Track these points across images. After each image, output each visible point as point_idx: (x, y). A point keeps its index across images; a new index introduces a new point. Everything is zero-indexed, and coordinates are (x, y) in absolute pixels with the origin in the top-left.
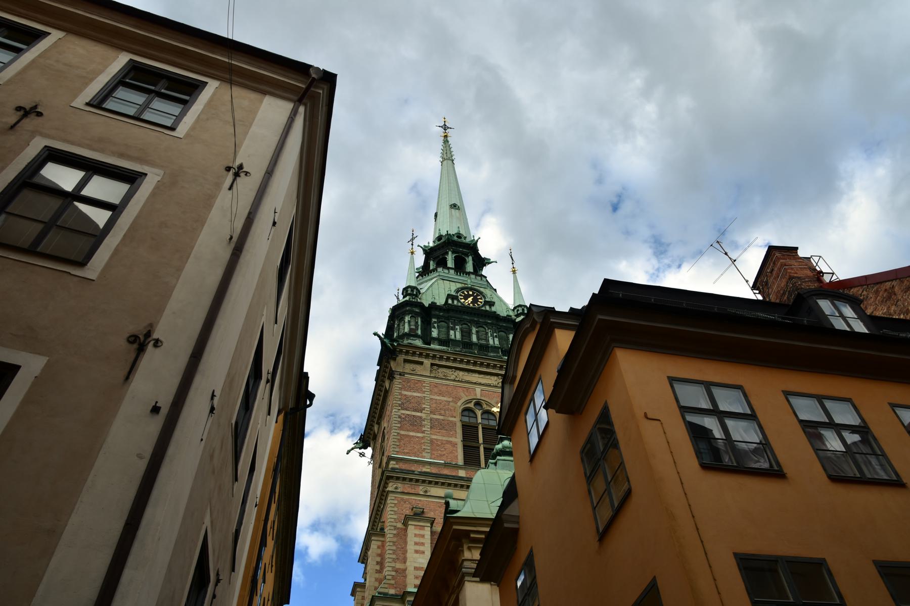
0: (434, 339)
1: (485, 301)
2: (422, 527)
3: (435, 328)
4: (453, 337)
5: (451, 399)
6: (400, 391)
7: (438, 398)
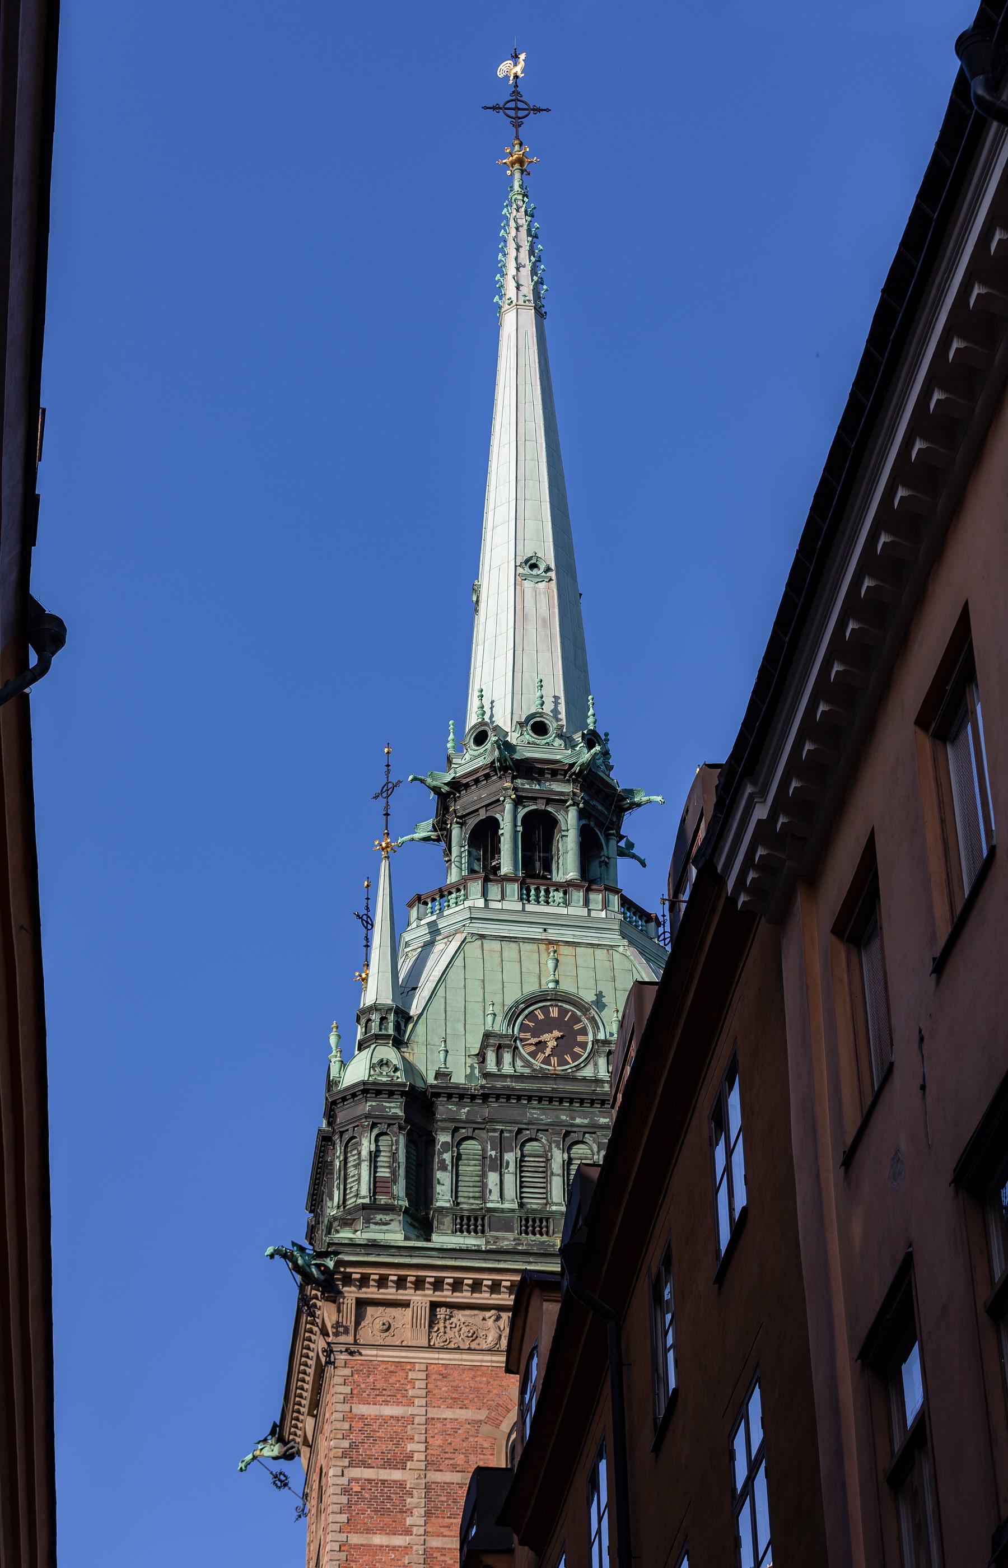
0: (442, 1209)
1: (596, 1041)
3: (443, 1168)
5: (482, 1415)
6: (346, 1407)
7: (448, 1414)
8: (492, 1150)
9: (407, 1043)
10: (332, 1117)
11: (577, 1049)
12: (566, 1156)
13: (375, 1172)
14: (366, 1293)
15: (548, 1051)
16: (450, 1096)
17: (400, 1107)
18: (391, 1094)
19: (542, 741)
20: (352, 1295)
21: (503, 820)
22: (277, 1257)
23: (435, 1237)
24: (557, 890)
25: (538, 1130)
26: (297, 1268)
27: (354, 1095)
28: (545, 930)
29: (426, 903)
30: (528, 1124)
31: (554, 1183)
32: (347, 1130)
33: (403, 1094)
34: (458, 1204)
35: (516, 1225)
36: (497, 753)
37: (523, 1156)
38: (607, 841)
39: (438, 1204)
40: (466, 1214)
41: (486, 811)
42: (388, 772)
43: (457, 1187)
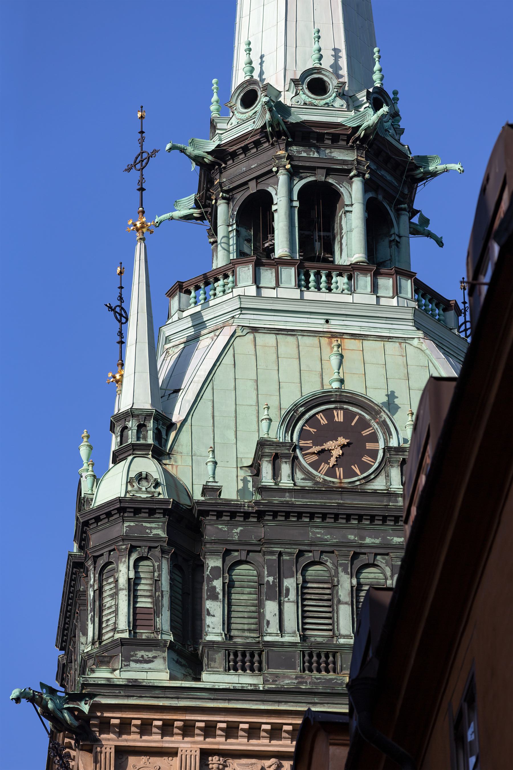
1: (387, 449)
3: (214, 597)
8: (269, 575)
9: (169, 454)
10: (84, 540)
11: (366, 459)
12: (354, 581)
13: (135, 602)
14: (127, 740)
15: (332, 461)
16: (219, 514)
17: (162, 528)
18: (152, 512)
19: (320, 101)
20: (111, 743)
21: (276, 194)
22: (23, 701)
23: (205, 676)
24: (340, 275)
25: (322, 552)
26: (47, 714)
27: (109, 515)
28: (327, 321)
29: (189, 292)
30: (311, 545)
31: (341, 613)
32: (102, 555)
33: (166, 512)
34: (231, 638)
35: (298, 661)
36: (268, 116)
37: (305, 581)
38: (398, 216)
39: (209, 638)
40: (240, 649)
41: (257, 183)
42: (143, 139)
43: (229, 618)
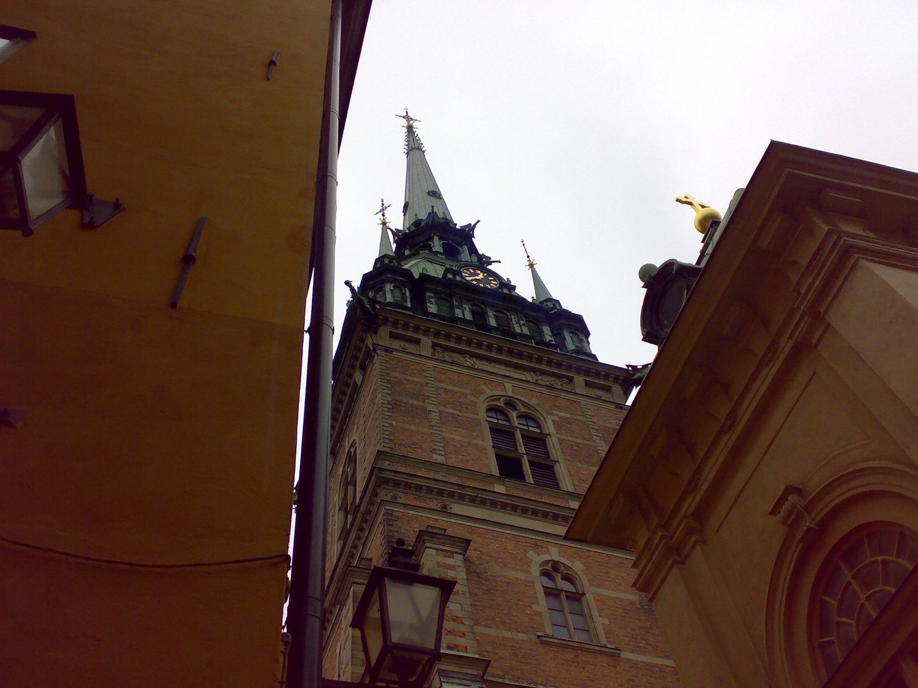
2: (451, 554)
4: (461, 316)
5: (468, 391)
